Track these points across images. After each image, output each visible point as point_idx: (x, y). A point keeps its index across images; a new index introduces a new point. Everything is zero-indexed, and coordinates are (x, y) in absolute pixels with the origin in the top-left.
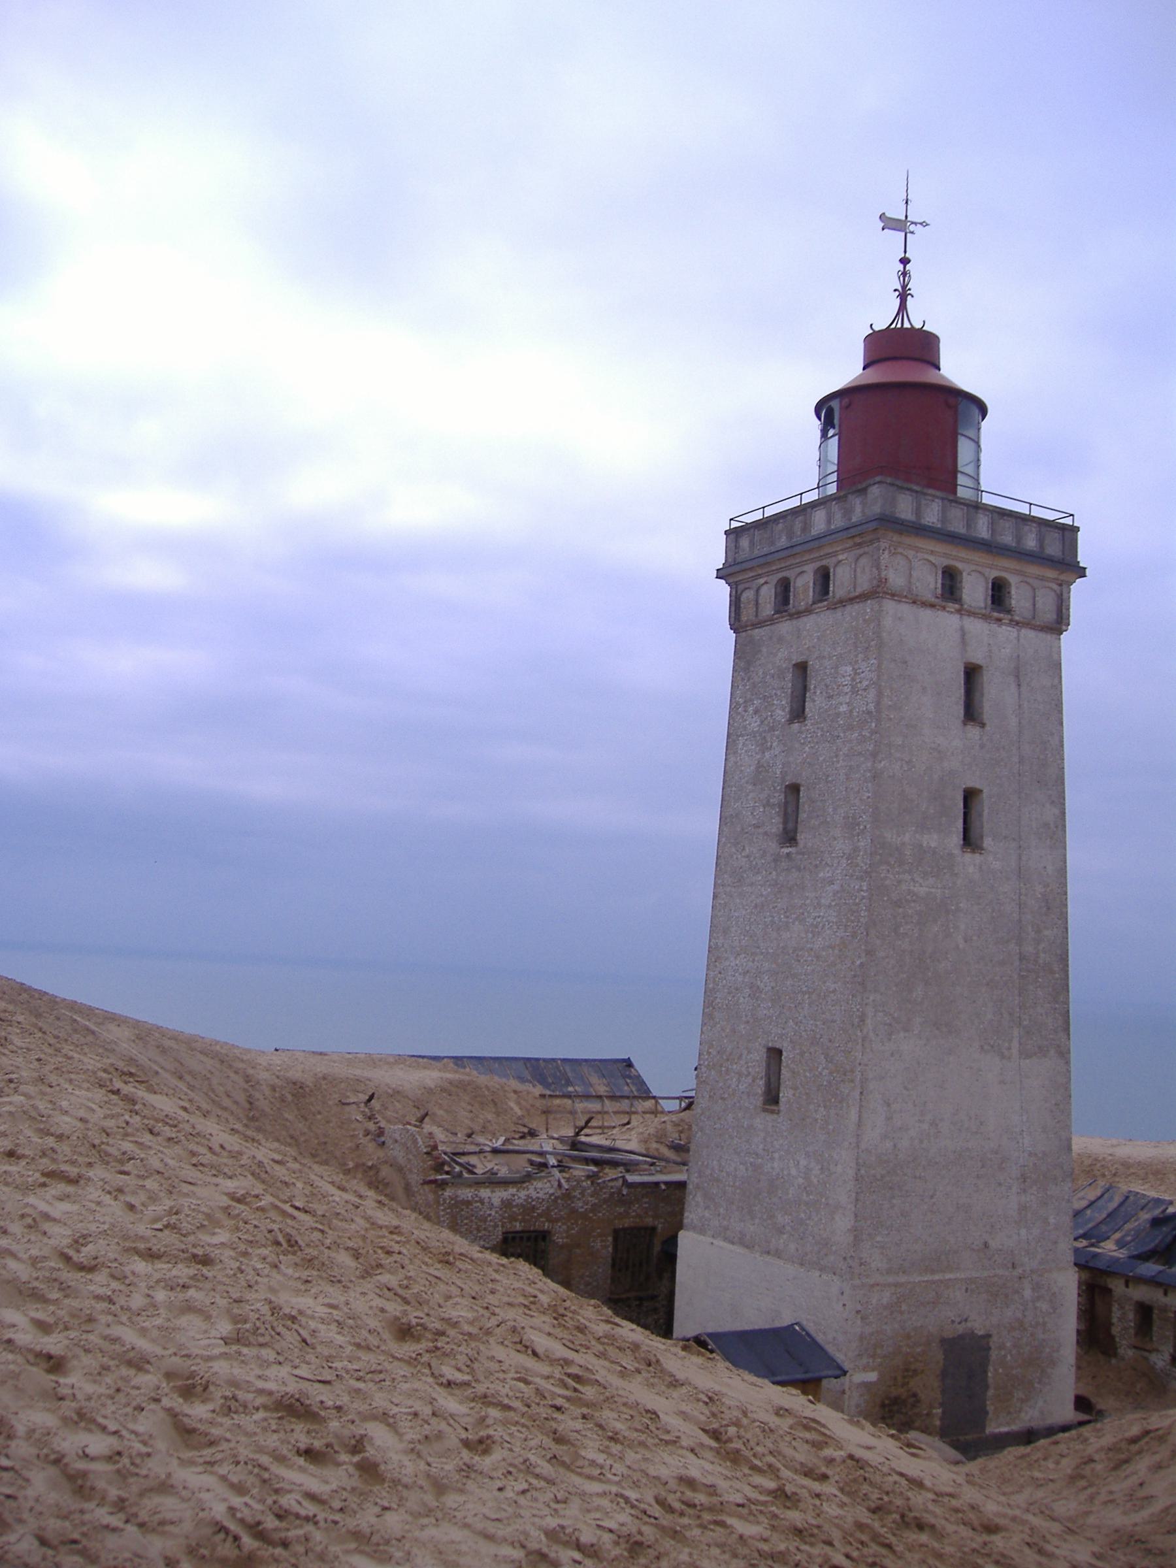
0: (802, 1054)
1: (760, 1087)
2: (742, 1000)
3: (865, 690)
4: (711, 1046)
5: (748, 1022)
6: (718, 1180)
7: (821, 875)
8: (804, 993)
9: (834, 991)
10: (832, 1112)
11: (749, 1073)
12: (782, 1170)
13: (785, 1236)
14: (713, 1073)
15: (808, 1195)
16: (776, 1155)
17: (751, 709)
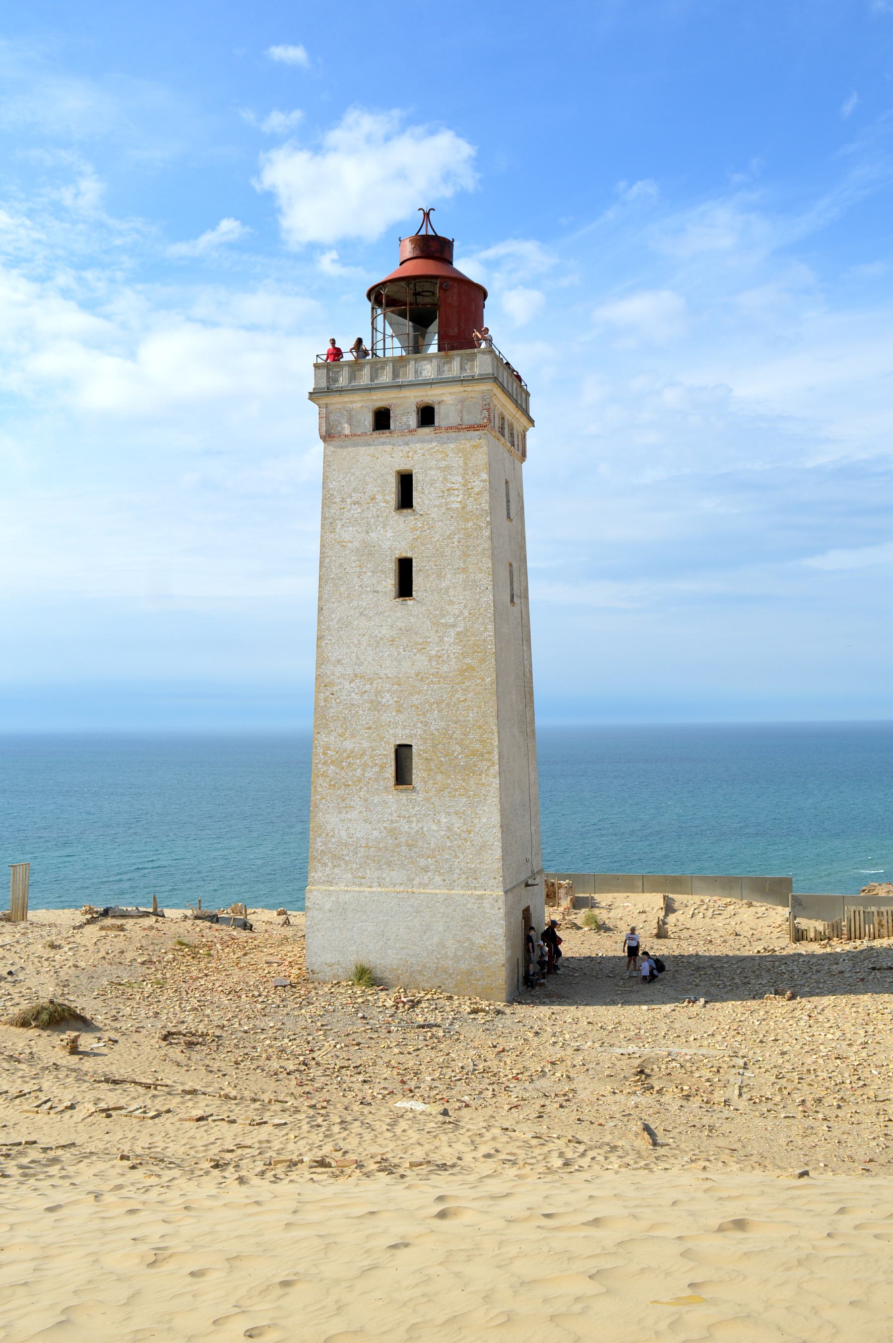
0: (435, 746)
2: (361, 712)
3: (478, 494)
5: (370, 728)
6: (345, 845)
7: (443, 621)
8: (431, 704)
9: (465, 701)
10: (472, 782)
11: (376, 765)
13: (429, 874)
14: (332, 767)
16: (414, 819)
17: (349, 501)
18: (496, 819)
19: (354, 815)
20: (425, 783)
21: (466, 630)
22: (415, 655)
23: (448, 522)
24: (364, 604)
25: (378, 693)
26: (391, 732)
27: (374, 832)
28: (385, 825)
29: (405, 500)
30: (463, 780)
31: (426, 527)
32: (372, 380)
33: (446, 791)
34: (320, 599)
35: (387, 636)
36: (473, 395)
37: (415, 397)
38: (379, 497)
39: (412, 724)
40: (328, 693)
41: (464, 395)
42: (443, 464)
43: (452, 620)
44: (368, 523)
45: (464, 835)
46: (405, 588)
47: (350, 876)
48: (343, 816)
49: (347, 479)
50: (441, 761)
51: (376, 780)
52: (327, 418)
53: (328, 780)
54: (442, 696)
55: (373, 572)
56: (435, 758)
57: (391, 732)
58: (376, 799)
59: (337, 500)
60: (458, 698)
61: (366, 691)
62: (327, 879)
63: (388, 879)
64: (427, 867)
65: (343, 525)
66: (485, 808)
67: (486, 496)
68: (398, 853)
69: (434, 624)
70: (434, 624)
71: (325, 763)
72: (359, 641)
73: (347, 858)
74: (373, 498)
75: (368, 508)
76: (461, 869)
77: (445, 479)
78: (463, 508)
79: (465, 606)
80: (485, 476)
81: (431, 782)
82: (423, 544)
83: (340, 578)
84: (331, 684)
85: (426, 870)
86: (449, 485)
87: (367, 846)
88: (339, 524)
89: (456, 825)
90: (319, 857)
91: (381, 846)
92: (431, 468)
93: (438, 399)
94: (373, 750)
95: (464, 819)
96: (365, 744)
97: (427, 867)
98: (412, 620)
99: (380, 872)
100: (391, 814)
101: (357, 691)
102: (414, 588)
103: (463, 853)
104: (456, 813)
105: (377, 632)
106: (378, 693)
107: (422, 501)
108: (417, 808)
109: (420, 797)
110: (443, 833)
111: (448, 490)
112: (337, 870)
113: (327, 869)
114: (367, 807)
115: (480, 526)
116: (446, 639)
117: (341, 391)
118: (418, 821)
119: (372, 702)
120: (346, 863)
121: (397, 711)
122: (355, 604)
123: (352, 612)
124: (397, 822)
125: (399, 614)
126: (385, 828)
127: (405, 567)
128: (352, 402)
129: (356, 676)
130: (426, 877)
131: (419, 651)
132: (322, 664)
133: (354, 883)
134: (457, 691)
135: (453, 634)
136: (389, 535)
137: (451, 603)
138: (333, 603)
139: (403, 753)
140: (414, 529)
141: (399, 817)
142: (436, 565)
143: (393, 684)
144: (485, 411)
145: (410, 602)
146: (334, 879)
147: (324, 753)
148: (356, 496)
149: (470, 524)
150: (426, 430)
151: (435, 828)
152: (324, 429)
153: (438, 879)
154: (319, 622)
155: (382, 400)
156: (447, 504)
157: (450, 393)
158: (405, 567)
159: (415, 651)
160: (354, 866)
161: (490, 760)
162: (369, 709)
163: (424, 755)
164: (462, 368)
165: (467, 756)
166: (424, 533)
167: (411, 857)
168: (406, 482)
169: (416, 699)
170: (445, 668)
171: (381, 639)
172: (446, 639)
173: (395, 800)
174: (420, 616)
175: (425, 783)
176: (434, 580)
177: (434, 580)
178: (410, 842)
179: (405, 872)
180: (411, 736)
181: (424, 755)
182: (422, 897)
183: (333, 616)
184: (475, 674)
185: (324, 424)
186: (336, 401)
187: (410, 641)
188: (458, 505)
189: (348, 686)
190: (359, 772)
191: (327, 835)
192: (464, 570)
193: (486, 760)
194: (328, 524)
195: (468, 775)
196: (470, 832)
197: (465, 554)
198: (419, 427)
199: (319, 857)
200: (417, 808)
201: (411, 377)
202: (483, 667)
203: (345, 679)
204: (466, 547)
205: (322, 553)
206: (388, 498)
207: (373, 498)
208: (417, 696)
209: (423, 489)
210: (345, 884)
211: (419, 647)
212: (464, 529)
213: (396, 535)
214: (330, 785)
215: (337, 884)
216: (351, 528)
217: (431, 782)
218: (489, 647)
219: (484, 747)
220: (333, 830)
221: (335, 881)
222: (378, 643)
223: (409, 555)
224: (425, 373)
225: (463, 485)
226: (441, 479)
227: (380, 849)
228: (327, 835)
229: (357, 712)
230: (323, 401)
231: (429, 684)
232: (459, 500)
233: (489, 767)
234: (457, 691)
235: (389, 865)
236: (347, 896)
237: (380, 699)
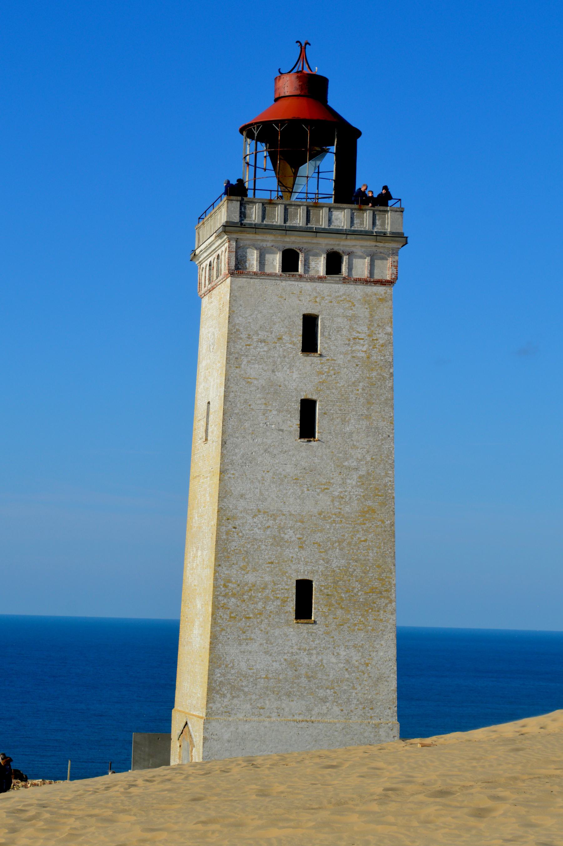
0: (336, 583)
1: (291, 606)
3: (382, 346)
4: (230, 581)
5: (272, 563)
7: (346, 464)
9: (365, 541)
10: (370, 618)
11: (278, 598)
12: (322, 660)
13: (328, 704)
14: (233, 600)
15: (349, 673)
16: (314, 652)
17: (255, 338)
18: (393, 652)
19: (254, 647)
20: (326, 617)
21: (368, 474)
22: (318, 494)
23: (353, 370)
24: (269, 441)
25: (281, 529)
26: (293, 567)
27: (274, 664)
28: (286, 657)
29: (309, 344)
30: (363, 615)
31: (332, 372)
33: (346, 626)
34: (224, 433)
35: (291, 475)
36: (381, 250)
37: (327, 244)
38: (286, 338)
39: (314, 561)
40: (230, 526)
41: (374, 249)
43: (355, 464)
44: (275, 363)
45: (362, 668)
46: (307, 429)
47: (249, 706)
48: (243, 647)
49: (254, 316)
50: (341, 597)
51: (278, 614)
52: (236, 252)
53: (228, 613)
54: (344, 536)
55: (279, 411)
56: (336, 594)
57: (293, 567)
58: (277, 632)
59: (244, 336)
60: (359, 538)
61: (269, 527)
62: (225, 710)
63: (287, 709)
64: (326, 697)
65: (249, 362)
66: (383, 642)
68: (298, 685)
69: (338, 466)
70: (338, 466)
71: (225, 596)
72: (263, 477)
73: (246, 689)
74: (280, 339)
75: (275, 347)
76: (358, 700)
77: (351, 328)
78: (368, 358)
79: (368, 452)
81: (331, 616)
82: (328, 389)
83: (245, 414)
84: (234, 518)
85: (324, 700)
86: (355, 334)
87: (267, 678)
88: (245, 361)
89: (355, 658)
90: (218, 688)
91: (281, 677)
92: (338, 316)
93: (348, 249)
94: (275, 584)
95: (362, 653)
96: (267, 578)
97: (326, 697)
98: (317, 461)
99: (279, 702)
100: (292, 647)
101: (260, 526)
103: (360, 684)
104: (355, 646)
105: (281, 470)
106: (281, 529)
107: (329, 347)
108: (317, 642)
109: (319, 629)
110: (342, 665)
111: (354, 339)
112: (235, 701)
113: (226, 700)
114: (267, 640)
115: (383, 376)
116: (349, 481)
118: (318, 654)
119: (274, 537)
120: (246, 694)
121: (300, 547)
122: (259, 440)
123: (256, 449)
124: (297, 654)
125: (304, 454)
126: (285, 660)
127: (308, 408)
128: (263, 241)
129: (259, 511)
130: (324, 707)
131: (323, 490)
132: (225, 497)
133: (253, 714)
134: (358, 531)
135: (355, 477)
136: (295, 376)
137: (354, 447)
138: (237, 438)
139: (304, 589)
140: (320, 373)
141: (299, 649)
142: (340, 410)
143: (296, 521)
144: (393, 268)
145: (313, 443)
146: (232, 709)
147: (225, 586)
149: (374, 374)
150: (335, 277)
151: (334, 660)
152: (233, 263)
153: (336, 709)
154: (223, 456)
155: (294, 242)
156: (353, 352)
157: (362, 246)
158: (308, 408)
159: (318, 490)
160: (254, 697)
161: (388, 597)
162: (272, 544)
163: (325, 591)
165: (366, 593)
166: (330, 378)
167: (311, 688)
169: (318, 537)
170: (347, 509)
171: (285, 477)
172: (349, 481)
173: (295, 632)
174: (324, 457)
175: (326, 617)
176: (338, 424)
177: (338, 424)
178: (310, 674)
179: (303, 702)
180: (313, 572)
181: (325, 591)
182: (321, 726)
183: (237, 451)
184: (375, 516)
185: (233, 259)
186: (247, 237)
187: (313, 481)
188: (363, 354)
189: (250, 521)
190: (260, 605)
191: (226, 666)
192: (368, 417)
193: (384, 597)
195: (367, 611)
196: (367, 665)
198: (328, 273)
199: (218, 688)
200: (317, 642)
201: (324, 224)
202: (383, 510)
203: (247, 514)
204: (370, 395)
206: (295, 340)
207: (280, 339)
208: (319, 534)
209: (329, 335)
210: (243, 715)
211: (323, 487)
212: (369, 378)
213: (301, 376)
214: (231, 617)
215: (235, 714)
216: (257, 366)
217: (331, 616)
218: (390, 491)
219: (383, 585)
220: (232, 661)
221: (234, 712)
222: (282, 481)
223: (314, 398)
225: (369, 336)
226: (347, 327)
227: (280, 681)
228: (226, 666)
229: (260, 546)
230: (235, 236)
231: (331, 523)
232: (364, 349)
233: (386, 604)
234: (358, 531)
235: (289, 696)
236: (247, 726)
237: (282, 535)
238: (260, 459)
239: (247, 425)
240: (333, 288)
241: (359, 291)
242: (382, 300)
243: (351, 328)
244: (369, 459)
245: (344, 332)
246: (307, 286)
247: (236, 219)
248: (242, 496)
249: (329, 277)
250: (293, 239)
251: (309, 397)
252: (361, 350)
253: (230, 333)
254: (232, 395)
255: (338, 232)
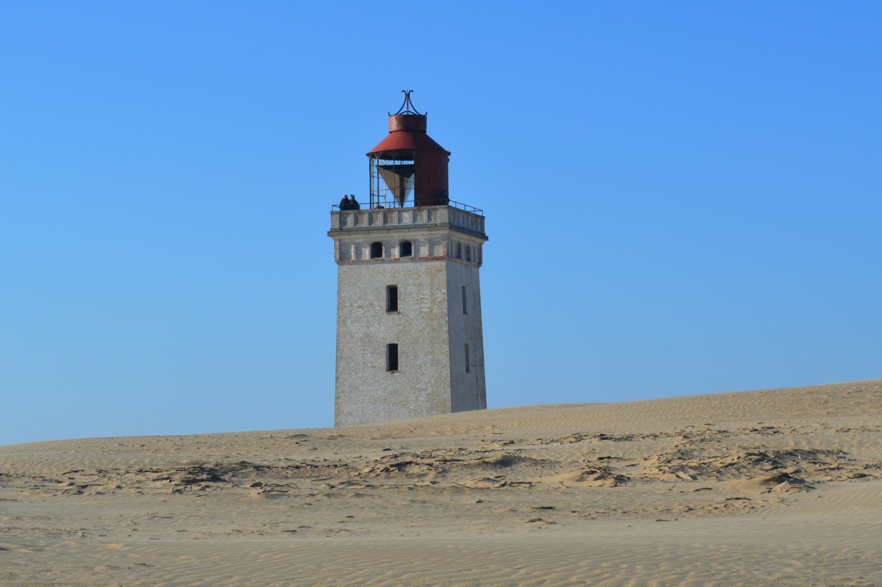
21: (433, 392)
24: (366, 375)
29: (393, 305)
32: (370, 224)
34: (337, 371)
38: (375, 303)
42: (418, 282)
44: (368, 321)
46: (393, 364)
52: (340, 249)
55: (372, 354)
59: (348, 305)
67: (445, 304)
74: (371, 304)
77: (419, 292)
80: (445, 291)
93: (414, 238)
98: (398, 386)
102: (399, 365)
117: (349, 231)
122: (360, 375)
127: (393, 350)
137: (423, 374)
145: (396, 374)
148: (360, 302)
150: (406, 258)
152: (338, 256)
154: (337, 387)
156: (420, 308)
158: (393, 350)
164: (429, 219)
168: (393, 292)
186: (346, 238)
192: (432, 353)
194: (341, 321)
197: (431, 342)
204: (434, 338)
205: (338, 340)
206: (381, 304)
213: (386, 328)
224: (404, 221)
230: (337, 238)
238: (361, 388)
239: (352, 365)
240: (406, 266)
241: (423, 266)
242: (439, 271)
243: (419, 292)
244: (433, 381)
245: (414, 296)
246: (388, 266)
247: (337, 226)
248: (350, 413)
249: (402, 259)
250: (375, 235)
251: (392, 342)
252: (426, 307)
253: (339, 303)
254: (341, 345)
255: (408, 228)
